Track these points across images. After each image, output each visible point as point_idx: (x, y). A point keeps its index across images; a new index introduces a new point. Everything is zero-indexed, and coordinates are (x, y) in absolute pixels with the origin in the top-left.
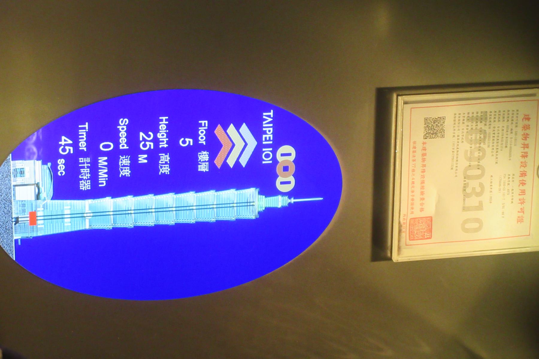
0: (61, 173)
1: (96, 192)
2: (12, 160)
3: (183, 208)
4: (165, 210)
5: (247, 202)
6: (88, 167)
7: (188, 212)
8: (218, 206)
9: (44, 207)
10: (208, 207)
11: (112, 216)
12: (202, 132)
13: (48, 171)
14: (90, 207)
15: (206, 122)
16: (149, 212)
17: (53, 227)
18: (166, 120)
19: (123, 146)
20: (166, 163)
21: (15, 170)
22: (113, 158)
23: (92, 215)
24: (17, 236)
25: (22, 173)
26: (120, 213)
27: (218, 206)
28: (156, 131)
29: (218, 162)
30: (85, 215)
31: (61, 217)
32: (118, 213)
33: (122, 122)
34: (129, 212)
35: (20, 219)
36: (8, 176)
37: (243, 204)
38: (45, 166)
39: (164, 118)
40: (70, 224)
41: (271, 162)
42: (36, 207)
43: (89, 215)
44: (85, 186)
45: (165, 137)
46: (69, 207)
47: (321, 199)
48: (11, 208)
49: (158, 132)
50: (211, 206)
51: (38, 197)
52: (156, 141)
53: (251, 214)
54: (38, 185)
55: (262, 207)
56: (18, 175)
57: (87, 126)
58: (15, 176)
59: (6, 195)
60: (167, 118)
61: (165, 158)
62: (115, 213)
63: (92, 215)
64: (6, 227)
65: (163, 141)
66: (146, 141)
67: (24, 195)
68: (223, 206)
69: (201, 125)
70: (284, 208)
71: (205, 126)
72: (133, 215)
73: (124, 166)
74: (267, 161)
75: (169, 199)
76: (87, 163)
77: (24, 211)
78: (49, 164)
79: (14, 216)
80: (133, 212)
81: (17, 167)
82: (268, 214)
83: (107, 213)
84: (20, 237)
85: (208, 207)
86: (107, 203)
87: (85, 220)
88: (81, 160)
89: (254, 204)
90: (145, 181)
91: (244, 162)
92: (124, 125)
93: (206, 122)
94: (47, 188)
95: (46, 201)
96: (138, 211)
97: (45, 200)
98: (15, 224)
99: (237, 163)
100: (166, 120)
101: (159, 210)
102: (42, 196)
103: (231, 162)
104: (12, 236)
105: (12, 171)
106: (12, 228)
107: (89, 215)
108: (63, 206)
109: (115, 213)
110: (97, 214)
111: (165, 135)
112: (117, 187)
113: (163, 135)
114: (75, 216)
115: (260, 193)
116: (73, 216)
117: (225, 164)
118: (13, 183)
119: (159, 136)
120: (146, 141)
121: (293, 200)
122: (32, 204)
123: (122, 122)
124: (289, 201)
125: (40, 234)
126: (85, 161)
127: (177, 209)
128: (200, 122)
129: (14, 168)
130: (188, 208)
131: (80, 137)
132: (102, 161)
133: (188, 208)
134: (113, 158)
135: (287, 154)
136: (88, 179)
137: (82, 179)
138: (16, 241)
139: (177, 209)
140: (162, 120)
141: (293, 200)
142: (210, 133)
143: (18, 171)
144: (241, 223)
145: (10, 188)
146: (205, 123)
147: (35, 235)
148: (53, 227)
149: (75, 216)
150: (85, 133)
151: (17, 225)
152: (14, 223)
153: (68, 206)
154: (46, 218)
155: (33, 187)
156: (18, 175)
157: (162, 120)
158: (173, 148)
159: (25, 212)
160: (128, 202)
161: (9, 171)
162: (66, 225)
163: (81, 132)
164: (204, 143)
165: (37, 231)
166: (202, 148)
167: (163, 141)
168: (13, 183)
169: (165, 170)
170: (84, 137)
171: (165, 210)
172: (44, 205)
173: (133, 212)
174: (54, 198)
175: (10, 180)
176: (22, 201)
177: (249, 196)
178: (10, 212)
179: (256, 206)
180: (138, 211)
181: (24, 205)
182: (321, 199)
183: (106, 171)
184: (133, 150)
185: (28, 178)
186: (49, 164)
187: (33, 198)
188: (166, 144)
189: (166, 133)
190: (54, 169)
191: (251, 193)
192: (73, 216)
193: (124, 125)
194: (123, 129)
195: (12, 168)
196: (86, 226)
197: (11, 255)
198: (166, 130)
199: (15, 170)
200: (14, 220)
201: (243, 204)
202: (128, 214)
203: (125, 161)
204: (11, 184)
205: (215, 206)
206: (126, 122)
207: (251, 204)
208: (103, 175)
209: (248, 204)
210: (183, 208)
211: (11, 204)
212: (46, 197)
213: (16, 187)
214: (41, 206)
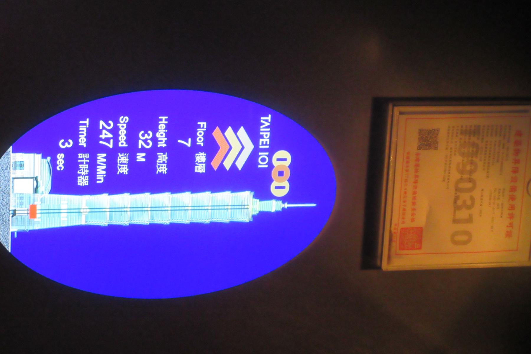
0: (60, 168)
1: (93, 188)
2: (13, 152)
3: (178, 208)
4: (160, 209)
5: (242, 205)
6: (87, 163)
7: (183, 211)
8: (213, 208)
9: (41, 200)
10: (203, 208)
11: (108, 213)
12: (200, 134)
13: (47, 165)
14: (87, 204)
15: (205, 123)
16: (145, 211)
17: (49, 221)
18: (166, 120)
19: (122, 144)
20: (164, 163)
21: (15, 163)
23: (88, 210)
24: (14, 229)
25: (21, 166)
26: (116, 210)
27: (213, 208)
28: (155, 130)
29: (215, 164)
30: (82, 211)
31: (59, 211)
32: (114, 210)
33: (122, 120)
34: (125, 209)
35: (17, 212)
37: (238, 207)
38: (45, 160)
39: (164, 118)
40: (66, 219)
41: (267, 166)
42: (34, 201)
43: (85, 210)
44: (83, 181)
45: (164, 136)
46: (66, 202)
47: (314, 205)
48: (9, 201)
49: (158, 131)
50: (206, 208)
51: (36, 190)
52: (155, 140)
53: (245, 217)
54: (36, 179)
55: (256, 211)
56: (18, 168)
57: (87, 122)
58: (15, 169)
59: (5, 187)
60: (167, 117)
61: (163, 157)
62: (111, 210)
63: (88, 210)
64: (3, 219)
65: (162, 141)
66: (144, 139)
67: (22, 188)
68: (218, 208)
69: (199, 126)
70: (277, 213)
71: (203, 128)
72: (129, 213)
73: (122, 164)
74: (263, 165)
75: (165, 198)
76: (86, 159)
77: (22, 204)
78: (49, 158)
79: (12, 208)
80: (129, 210)
81: (17, 160)
82: (262, 218)
83: (104, 210)
84: (17, 230)
85: (203, 208)
87: (81, 215)
88: (80, 155)
89: (248, 207)
90: (142, 180)
91: (240, 165)
92: (124, 123)
93: (205, 123)
95: (43, 195)
96: (134, 209)
97: (43, 193)
98: (12, 217)
99: (234, 166)
100: (166, 120)
101: (155, 209)
102: (40, 189)
103: (228, 165)
104: (9, 229)
105: (11, 164)
106: (9, 220)
107: (85, 210)
108: (61, 201)
109: (111, 210)
110: (93, 210)
111: (164, 134)
112: (115, 184)
113: (162, 135)
114: (72, 211)
115: (255, 197)
116: (70, 211)
117: (221, 166)
118: (12, 176)
119: (158, 135)
120: (144, 139)
121: (286, 205)
122: (30, 197)
123: (122, 120)
124: (283, 206)
126: (84, 157)
127: (173, 209)
128: (199, 123)
129: (14, 161)
130: (183, 208)
131: (80, 133)
132: (101, 158)
133: (183, 208)
135: (283, 159)
136: (86, 175)
137: (80, 175)
138: (13, 233)
139: (173, 209)
140: (161, 120)
141: (286, 205)
142: (208, 135)
143: (18, 164)
144: (235, 226)
145: (9, 181)
146: (203, 125)
147: (31, 228)
148: (49, 221)
149: (72, 211)
150: (85, 130)
151: (15, 217)
152: (11, 215)
154: (43, 211)
155: (32, 180)
156: (18, 168)
157: (161, 120)
158: (172, 148)
159: (22, 205)
160: (125, 199)
161: (9, 163)
162: (62, 219)
163: (82, 128)
164: (202, 144)
165: (34, 225)
166: (199, 149)
167: (162, 141)
168: (12, 176)
169: (162, 169)
170: (85, 133)
171: (160, 209)
172: (42, 199)
173: (129, 210)
174: (51, 192)
175: (9, 173)
176: (20, 194)
177: (243, 199)
178: (8, 204)
179: (250, 210)
180: (134, 209)
181: (22, 198)
182: (314, 205)
183: (105, 167)
184: (132, 149)
185: (27, 171)
186: (49, 158)
187: (31, 191)
188: (165, 143)
189: (165, 132)
191: (246, 196)
192: (70, 211)
193: (124, 123)
194: (123, 127)
195: (12, 161)
196: (82, 222)
197: (6, 247)
198: (165, 129)
199: (15, 163)
200: (11, 212)
201: (238, 207)
202: (124, 211)
203: (123, 158)
204: (10, 177)
205: (210, 208)
206: (126, 120)
207: (246, 207)
208: (101, 173)
209: (243, 207)
210: (178, 208)
211: (9, 196)
212: (44, 190)
213: (15, 180)
214: (39, 200)
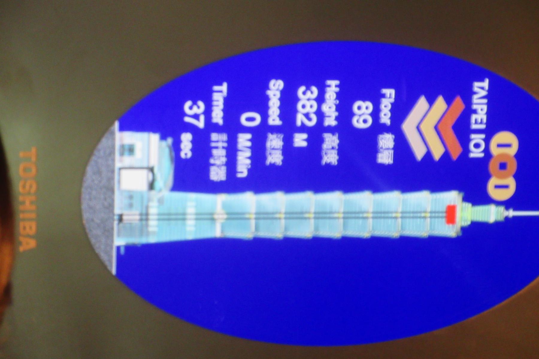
0: (186, 154)
1: (232, 185)
20: (333, 148)
22: (260, 135)
25: (131, 150)
36: (112, 153)
54: (151, 170)
58: (122, 154)
75: (334, 200)
78: (170, 140)
86: (248, 201)
88: (214, 136)
94: (165, 173)
112: (263, 179)
125: (152, 240)
126: (219, 140)
134: (260, 135)
145: (113, 171)
153: (193, 201)
160: (278, 201)
169: (331, 157)
175: (113, 160)
184: (288, 128)
186: (170, 140)
190: (176, 147)
196: (216, 232)
